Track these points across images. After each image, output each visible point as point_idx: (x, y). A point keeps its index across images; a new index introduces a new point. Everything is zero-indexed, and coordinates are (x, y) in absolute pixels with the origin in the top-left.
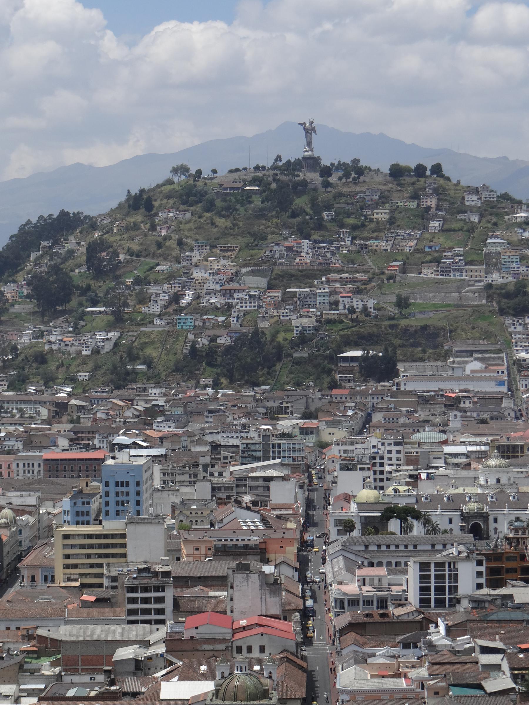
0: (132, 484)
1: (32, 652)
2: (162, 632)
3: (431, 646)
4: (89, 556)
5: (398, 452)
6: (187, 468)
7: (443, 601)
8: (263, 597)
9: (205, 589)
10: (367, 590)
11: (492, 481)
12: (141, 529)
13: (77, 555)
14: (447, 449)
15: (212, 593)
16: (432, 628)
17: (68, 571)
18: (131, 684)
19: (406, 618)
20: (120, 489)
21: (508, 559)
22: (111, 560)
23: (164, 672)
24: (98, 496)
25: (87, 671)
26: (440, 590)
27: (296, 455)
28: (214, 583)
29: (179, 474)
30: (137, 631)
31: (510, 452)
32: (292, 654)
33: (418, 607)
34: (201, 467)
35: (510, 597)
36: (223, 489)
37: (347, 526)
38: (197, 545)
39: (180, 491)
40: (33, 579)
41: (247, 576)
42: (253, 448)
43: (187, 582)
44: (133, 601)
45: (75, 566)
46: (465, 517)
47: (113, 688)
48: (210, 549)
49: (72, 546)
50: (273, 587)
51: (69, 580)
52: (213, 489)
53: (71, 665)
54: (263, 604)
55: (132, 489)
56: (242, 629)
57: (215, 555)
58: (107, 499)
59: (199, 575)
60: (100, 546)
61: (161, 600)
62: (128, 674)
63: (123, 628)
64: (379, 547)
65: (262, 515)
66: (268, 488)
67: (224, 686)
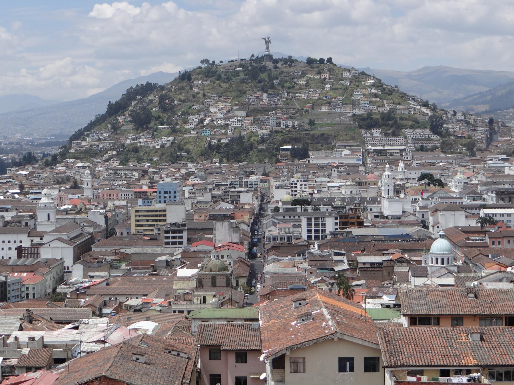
0: (172, 192)
1: (117, 260)
3: (310, 253)
4: (148, 221)
5: (305, 185)
7: (318, 236)
10: (282, 233)
11: (349, 192)
12: (173, 207)
14: (329, 184)
15: (206, 236)
16: (312, 247)
17: (138, 228)
19: (300, 244)
21: (351, 218)
22: (159, 223)
26: (317, 231)
27: (255, 187)
31: (360, 184)
32: (243, 259)
33: (306, 239)
38: (200, 215)
40: (122, 233)
44: (168, 238)
45: (141, 226)
49: (140, 216)
52: (212, 197)
55: (172, 195)
57: (209, 219)
58: (160, 199)
59: (201, 228)
60: (153, 216)
61: (181, 237)
62: (163, 267)
63: (162, 250)
64: (290, 217)
66: (239, 197)
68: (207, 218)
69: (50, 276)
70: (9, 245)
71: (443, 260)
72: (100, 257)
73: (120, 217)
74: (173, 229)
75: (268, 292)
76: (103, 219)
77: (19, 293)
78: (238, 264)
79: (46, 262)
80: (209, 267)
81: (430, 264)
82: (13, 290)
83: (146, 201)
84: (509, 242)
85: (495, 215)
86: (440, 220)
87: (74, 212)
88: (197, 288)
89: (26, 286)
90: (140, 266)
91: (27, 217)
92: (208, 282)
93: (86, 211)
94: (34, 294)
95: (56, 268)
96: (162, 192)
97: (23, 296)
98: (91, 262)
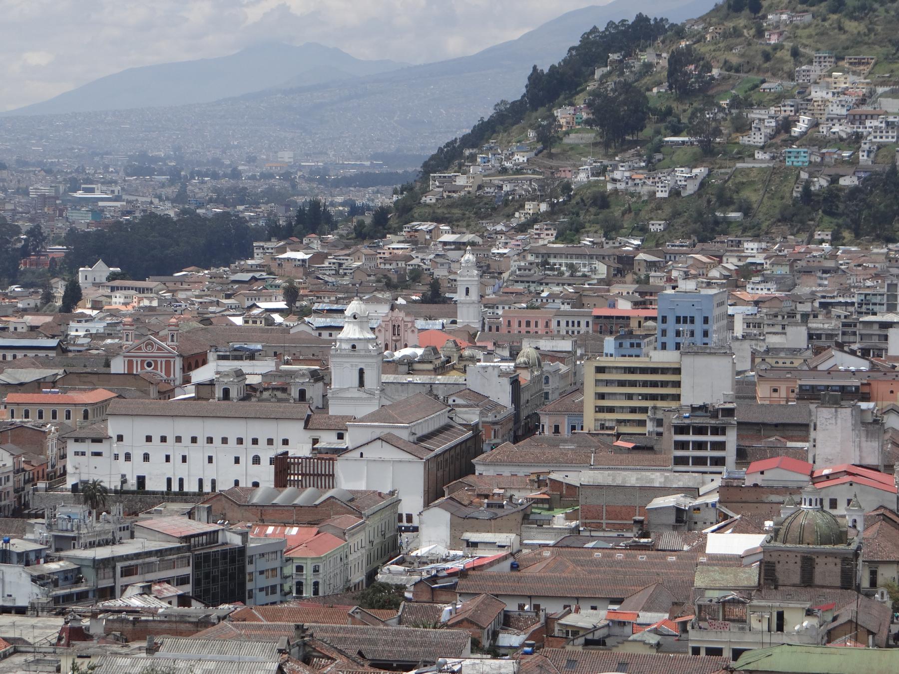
0: (699, 320)
1: (542, 501)
4: (630, 397)
6: (780, 318)
8: (858, 439)
9: (783, 440)
12: (701, 362)
13: (615, 394)
15: (790, 444)
22: (660, 404)
23: (715, 527)
24: (652, 338)
25: (614, 527)
28: (795, 433)
29: (768, 325)
32: (891, 511)
34: (798, 317)
36: (823, 337)
38: (776, 385)
39: (767, 340)
40: (557, 429)
41: (836, 411)
42: (874, 301)
43: (760, 431)
44: (682, 445)
45: (611, 410)
47: (643, 540)
48: (793, 391)
49: (608, 383)
50: (871, 427)
52: (810, 337)
53: (592, 519)
54: (857, 450)
55: (698, 327)
56: (825, 479)
58: (664, 339)
59: (775, 421)
60: (645, 384)
61: (721, 446)
62: (666, 526)
63: (666, 477)
65: (871, 362)
66: (886, 338)
67: (786, 524)
68: (793, 395)
69: (361, 538)
70: (254, 450)
72: (497, 491)
73: (554, 383)
74: (698, 421)
76: (509, 388)
77: (277, 581)
78: (877, 526)
79: (352, 500)
80: (795, 532)
82: (262, 573)
83: (627, 343)
87: (430, 367)
88: (759, 588)
89: (297, 563)
90: (604, 521)
91: (303, 375)
92: (790, 572)
93: (461, 366)
94: (316, 584)
95: (377, 518)
96: (671, 320)
97: (286, 588)
98: (471, 503)
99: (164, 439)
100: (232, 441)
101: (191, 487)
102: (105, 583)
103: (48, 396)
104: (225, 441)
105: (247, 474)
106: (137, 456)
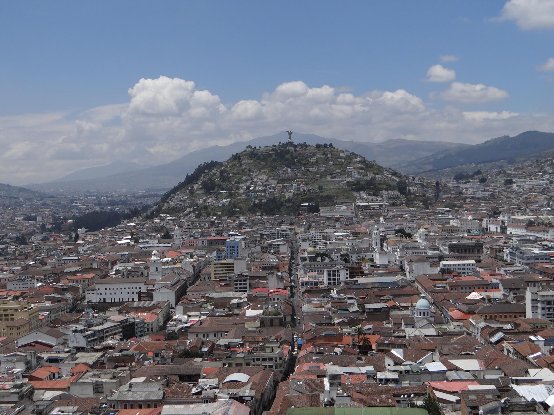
0: (236, 247)
2: (246, 294)
3: (332, 297)
4: (222, 270)
10: (311, 280)
12: (239, 261)
14: (336, 234)
16: (332, 291)
18: (236, 311)
20: (232, 249)
25: (222, 307)
26: (334, 279)
30: (238, 294)
31: (355, 235)
35: (357, 281)
37: (304, 259)
40: (204, 278)
44: (236, 284)
45: (218, 274)
46: (342, 256)
49: (217, 267)
51: (216, 278)
52: (261, 248)
53: (217, 305)
60: (226, 267)
61: (245, 284)
69: (161, 314)
71: (424, 313)
75: (311, 337)
76: (192, 268)
77: (143, 329)
80: (268, 313)
81: (416, 316)
84: (462, 289)
85: (450, 265)
86: (414, 268)
88: (260, 327)
96: (229, 248)
99: (110, 289)
100: (127, 288)
101: (117, 300)
102: (101, 336)
103: (79, 276)
104: (125, 288)
105: (131, 297)
106: (103, 294)
